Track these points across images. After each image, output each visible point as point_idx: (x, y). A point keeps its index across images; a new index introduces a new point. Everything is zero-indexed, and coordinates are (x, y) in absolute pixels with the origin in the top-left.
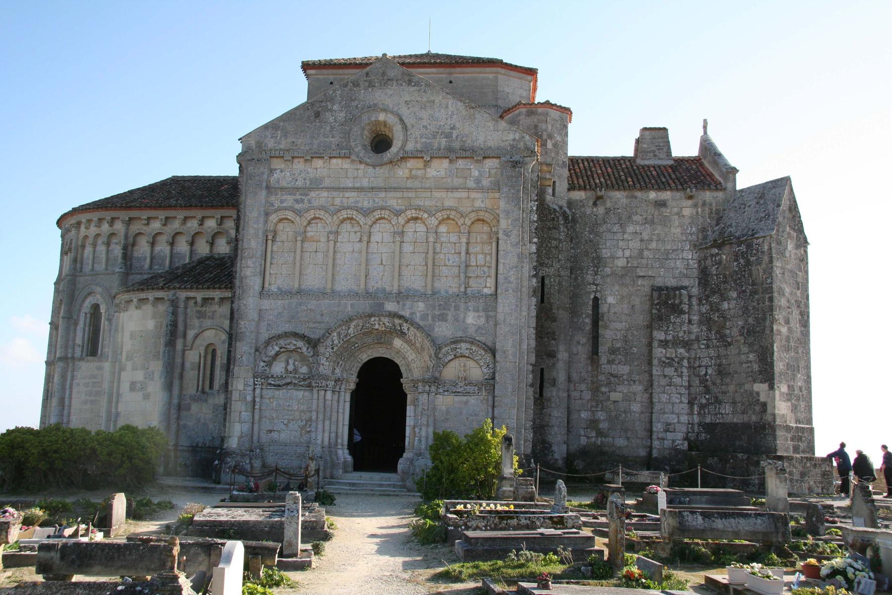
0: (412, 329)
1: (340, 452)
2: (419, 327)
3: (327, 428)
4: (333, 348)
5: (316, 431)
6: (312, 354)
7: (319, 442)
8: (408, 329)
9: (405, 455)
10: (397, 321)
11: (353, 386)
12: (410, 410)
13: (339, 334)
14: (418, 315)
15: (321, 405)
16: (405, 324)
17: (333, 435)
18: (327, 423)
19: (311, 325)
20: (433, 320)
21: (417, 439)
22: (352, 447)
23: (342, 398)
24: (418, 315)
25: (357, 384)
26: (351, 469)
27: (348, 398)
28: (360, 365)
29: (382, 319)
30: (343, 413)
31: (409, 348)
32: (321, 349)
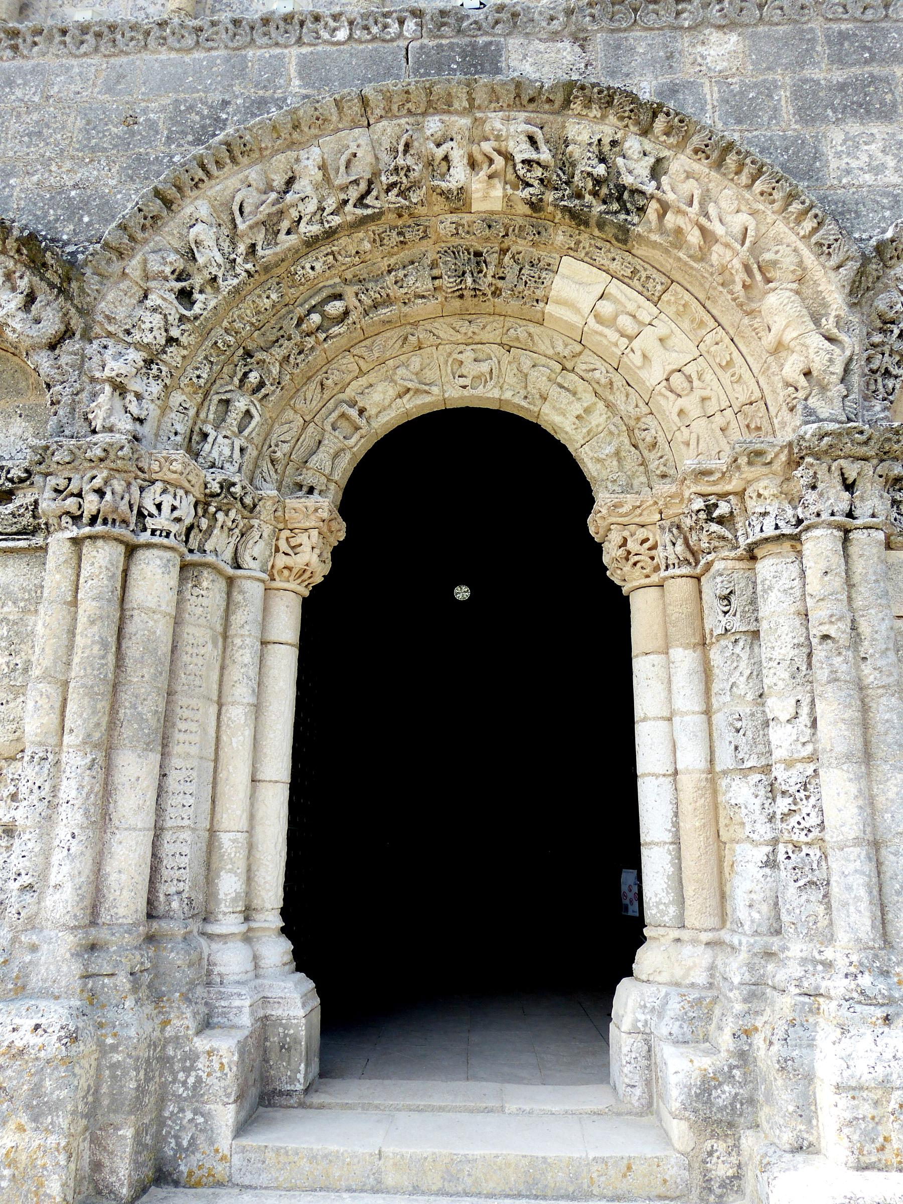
0: (680, 163)
1: (231, 960)
2: (719, 153)
3: (133, 804)
4: (185, 296)
5: (48, 820)
6: (51, 325)
7: (61, 901)
8: (657, 171)
9: (646, 959)
10: (583, 131)
11: (312, 559)
12: (661, 685)
13: (229, 218)
14: (711, 93)
15: (90, 638)
16: (633, 144)
17: (181, 851)
18: (135, 770)
19: (64, 175)
20: (808, 112)
21: (748, 859)
22: (315, 921)
23: (245, 618)
24: (711, 93)
25: (338, 553)
26: (297, 1073)
27: (287, 623)
28: (358, 445)
29: (495, 121)
30: (257, 709)
31: (647, 310)
32: (114, 302)
